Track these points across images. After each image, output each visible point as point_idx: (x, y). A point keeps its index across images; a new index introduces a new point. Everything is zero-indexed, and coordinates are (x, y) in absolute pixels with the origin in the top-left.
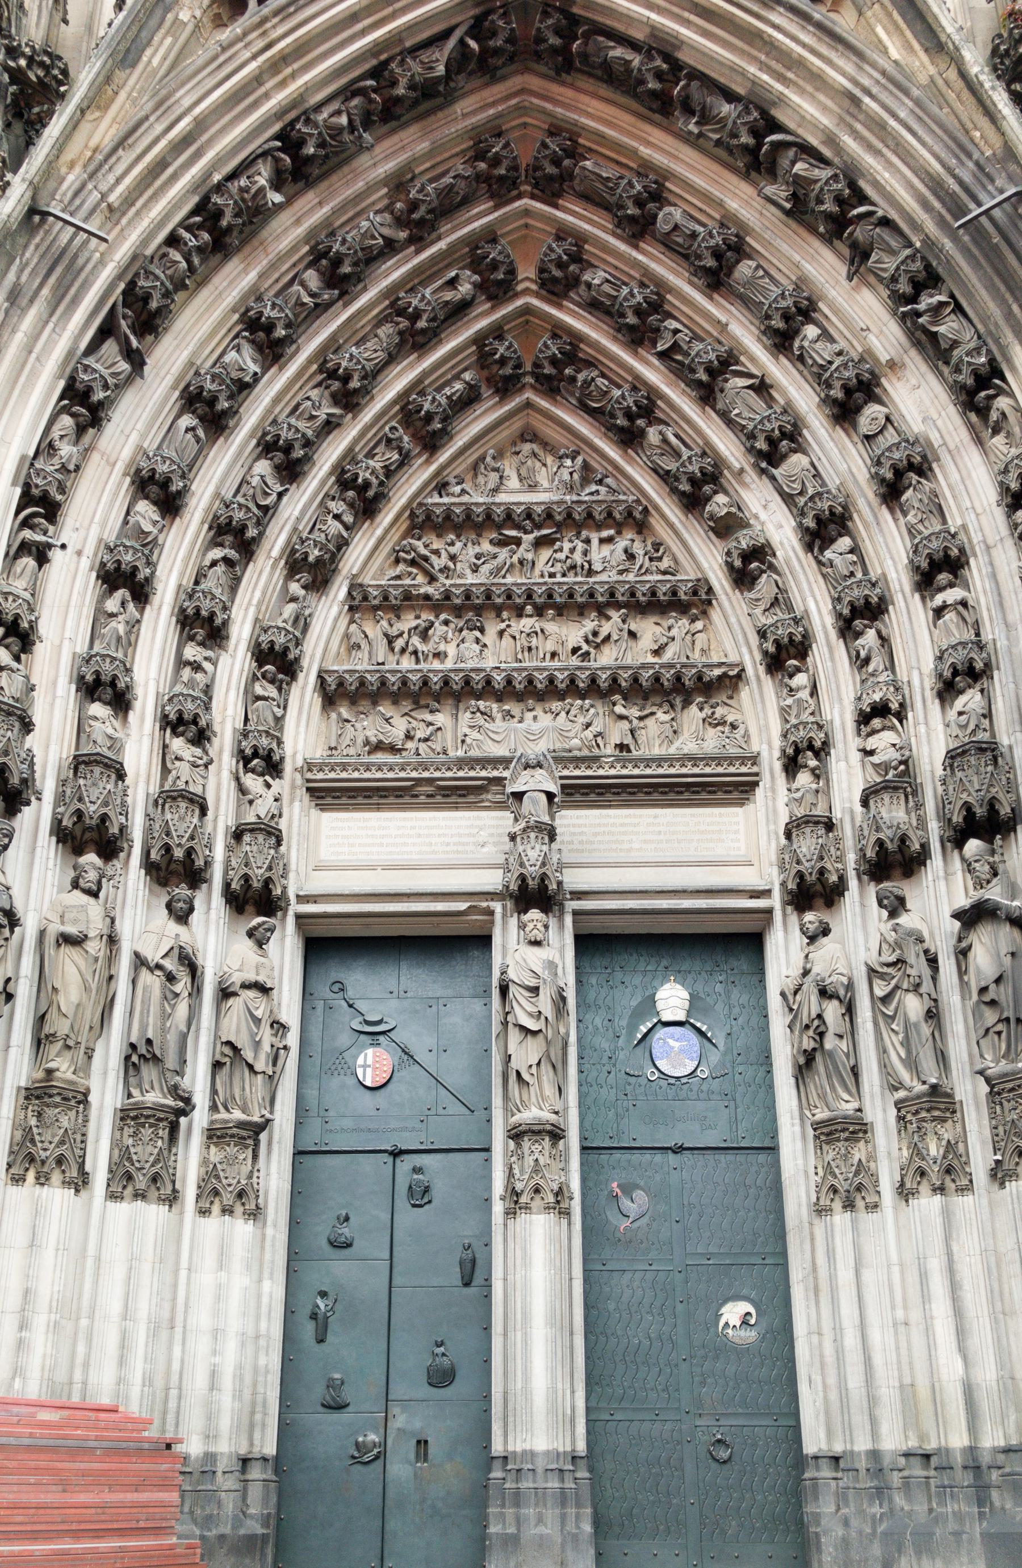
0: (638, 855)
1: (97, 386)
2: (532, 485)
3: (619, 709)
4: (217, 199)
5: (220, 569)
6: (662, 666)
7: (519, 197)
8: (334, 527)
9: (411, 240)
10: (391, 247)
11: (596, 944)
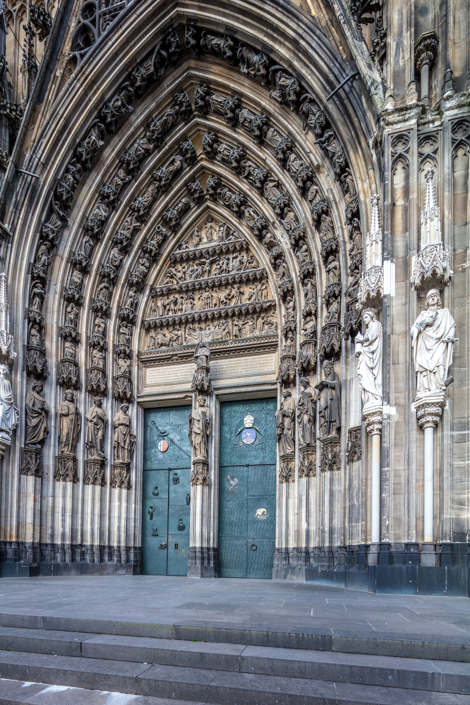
0: (238, 372)
1: (50, 233)
2: (209, 239)
3: (235, 322)
4: (80, 150)
5: (104, 290)
6: (249, 304)
7: (194, 117)
8: (142, 268)
9: (156, 147)
10: (148, 153)
11: (224, 403)
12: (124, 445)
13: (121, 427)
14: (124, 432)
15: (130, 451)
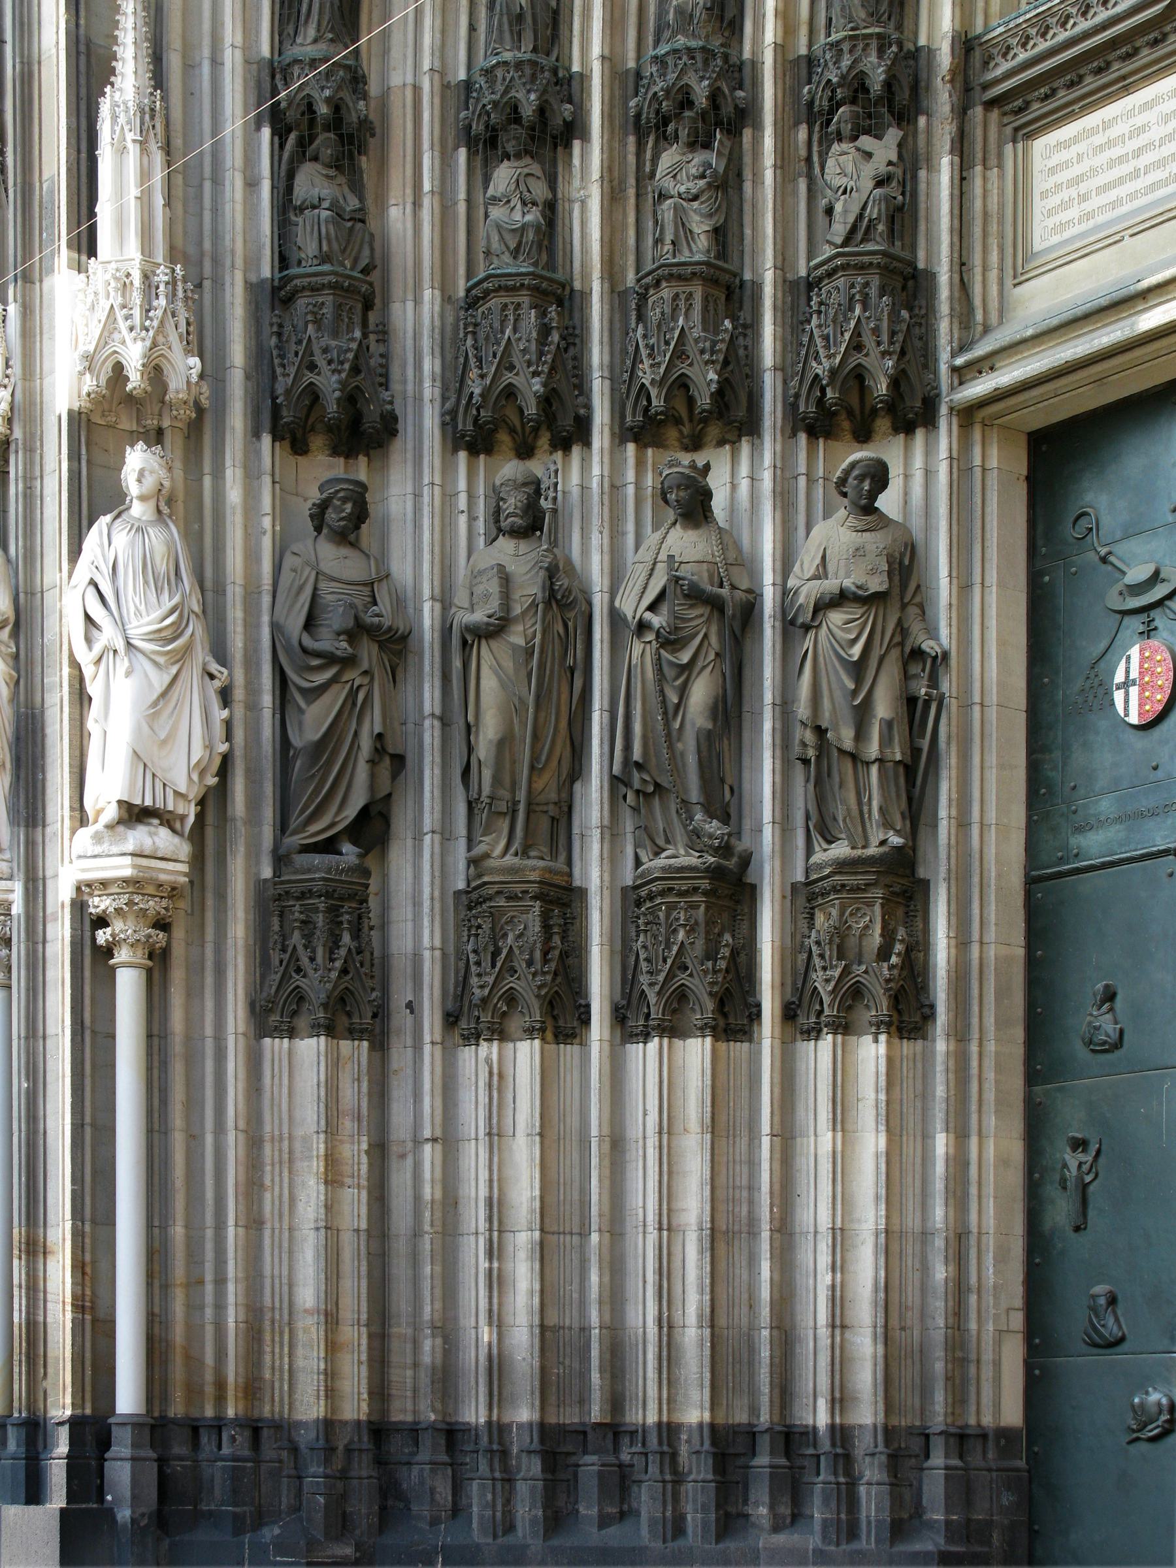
12: (861, 734)
13: (836, 617)
14: (856, 651)
15: (909, 769)
